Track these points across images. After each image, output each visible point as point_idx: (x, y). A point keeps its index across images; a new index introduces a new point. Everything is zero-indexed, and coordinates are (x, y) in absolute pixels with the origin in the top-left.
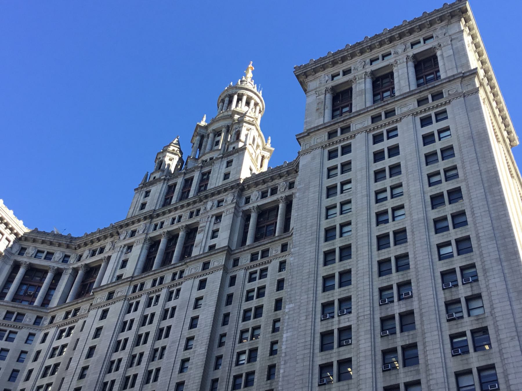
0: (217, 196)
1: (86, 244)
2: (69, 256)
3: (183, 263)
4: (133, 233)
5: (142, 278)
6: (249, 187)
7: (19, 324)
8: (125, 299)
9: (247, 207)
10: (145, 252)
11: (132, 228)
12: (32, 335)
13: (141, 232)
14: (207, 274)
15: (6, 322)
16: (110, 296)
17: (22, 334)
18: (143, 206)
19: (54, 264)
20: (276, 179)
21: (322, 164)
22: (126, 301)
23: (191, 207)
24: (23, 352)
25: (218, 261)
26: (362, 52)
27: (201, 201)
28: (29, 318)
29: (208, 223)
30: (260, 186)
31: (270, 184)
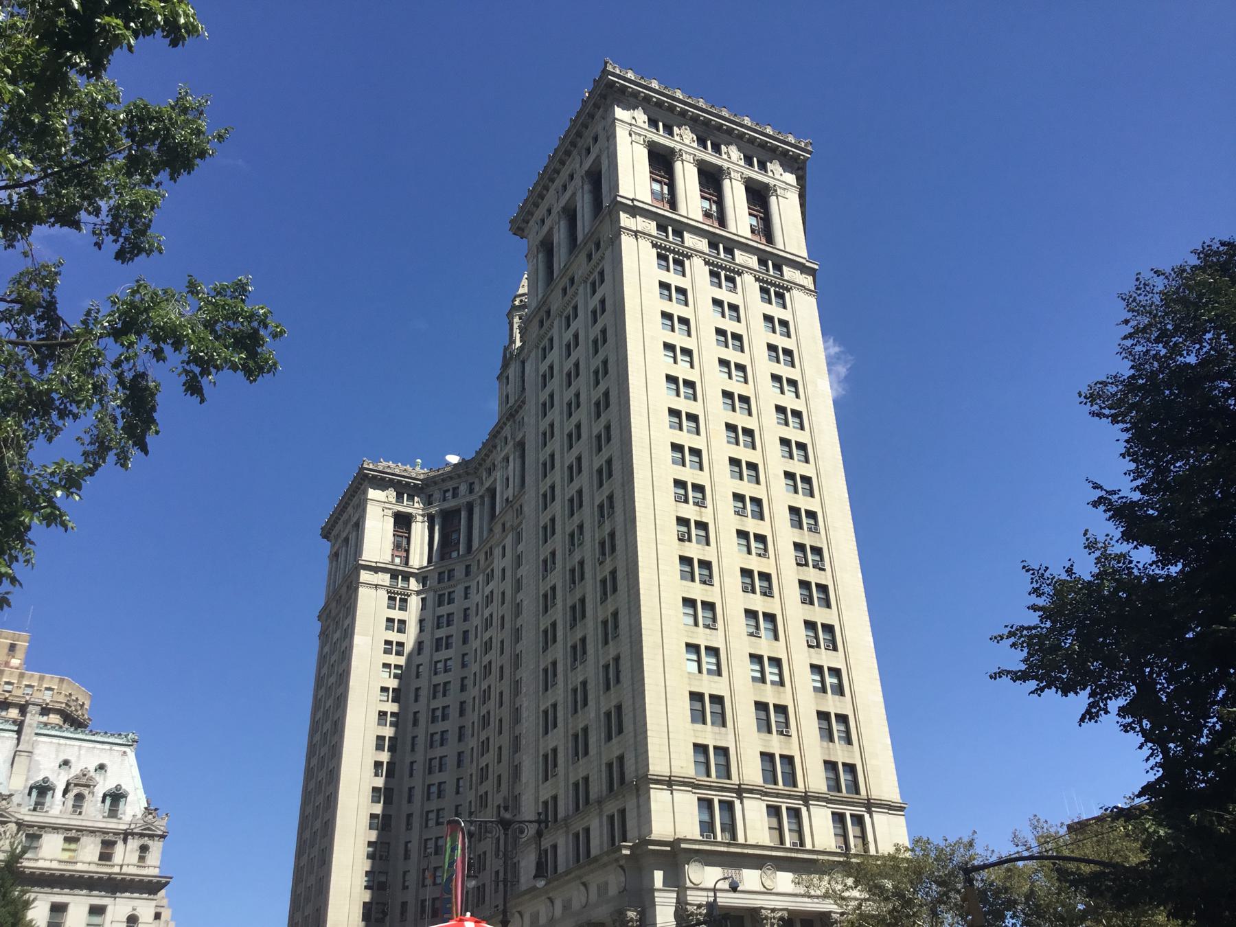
1: (480, 465)
2: (472, 484)
4: (506, 438)
7: (452, 583)
10: (518, 461)
11: (503, 433)
12: (467, 588)
15: (442, 585)
16: (504, 525)
17: (459, 591)
18: (507, 397)
19: (462, 500)
21: (537, 370)
24: (466, 610)
26: (552, 180)
28: (459, 572)
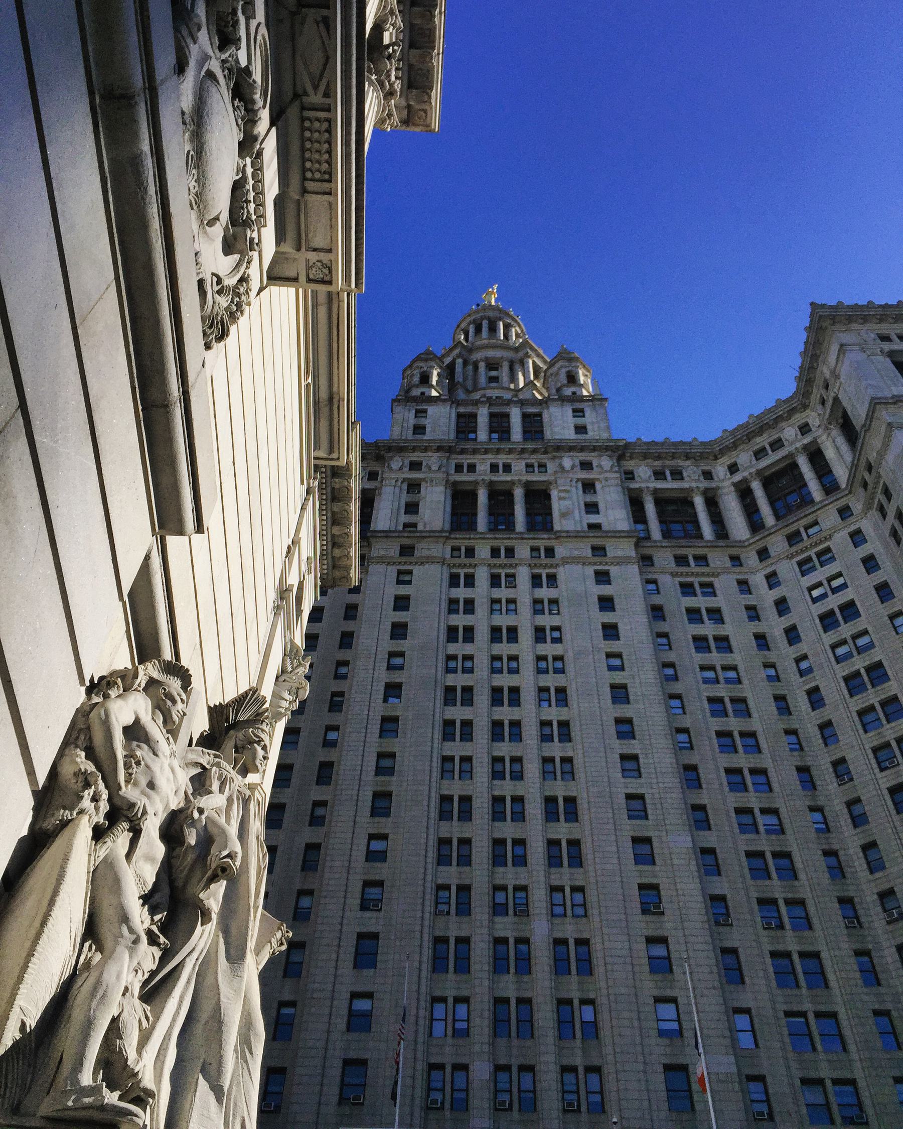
0: (579, 454)
3: (553, 536)
5: (470, 539)
6: (631, 458)
8: (443, 564)
9: (634, 485)
13: (435, 467)
14: (607, 564)
20: (679, 458)
22: (445, 567)
23: (526, 456)
25: (625, 549)
27: (546, 452)
29: (574, 489)
30: (649, 461)
31: (668, 463)
